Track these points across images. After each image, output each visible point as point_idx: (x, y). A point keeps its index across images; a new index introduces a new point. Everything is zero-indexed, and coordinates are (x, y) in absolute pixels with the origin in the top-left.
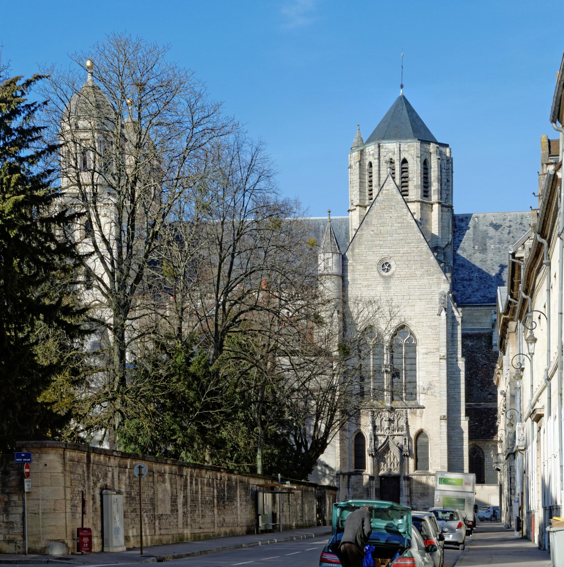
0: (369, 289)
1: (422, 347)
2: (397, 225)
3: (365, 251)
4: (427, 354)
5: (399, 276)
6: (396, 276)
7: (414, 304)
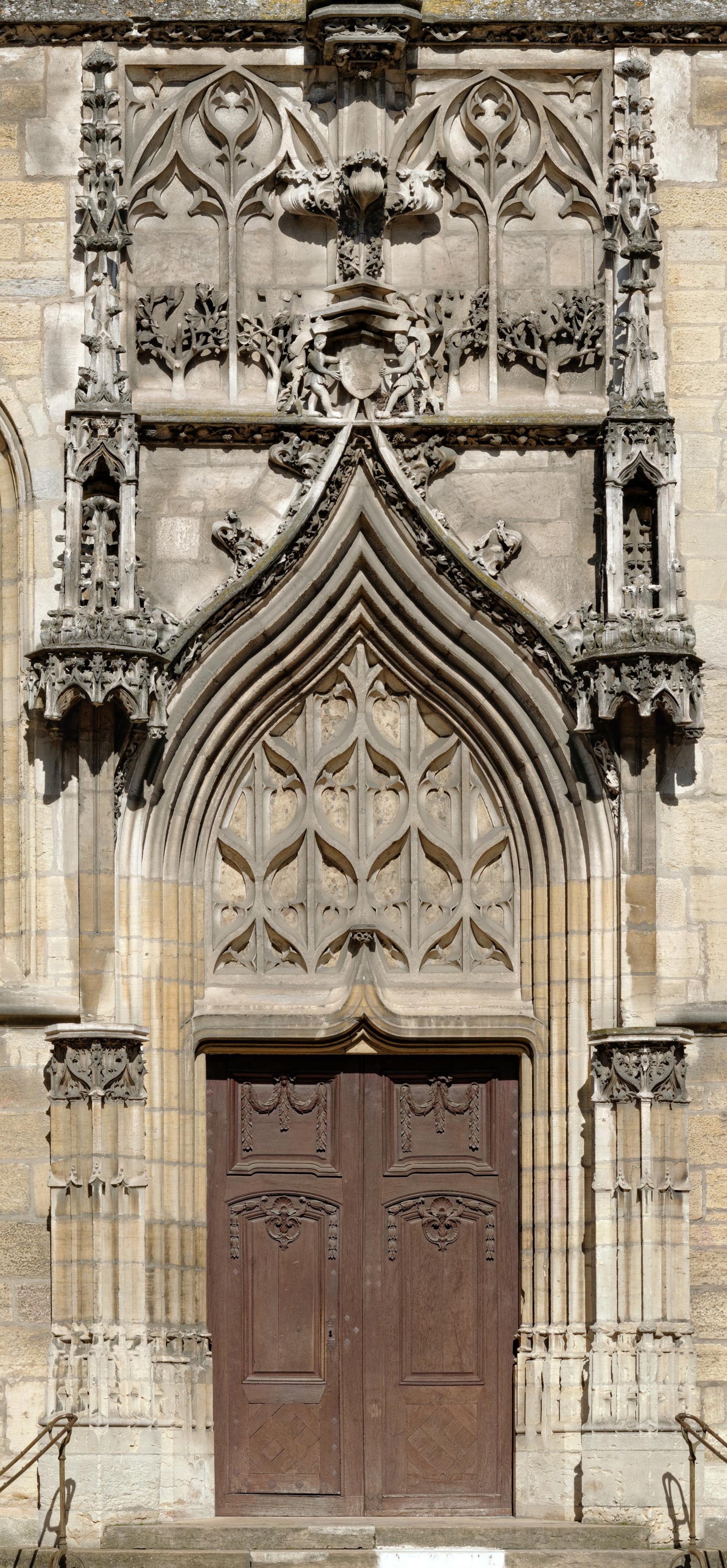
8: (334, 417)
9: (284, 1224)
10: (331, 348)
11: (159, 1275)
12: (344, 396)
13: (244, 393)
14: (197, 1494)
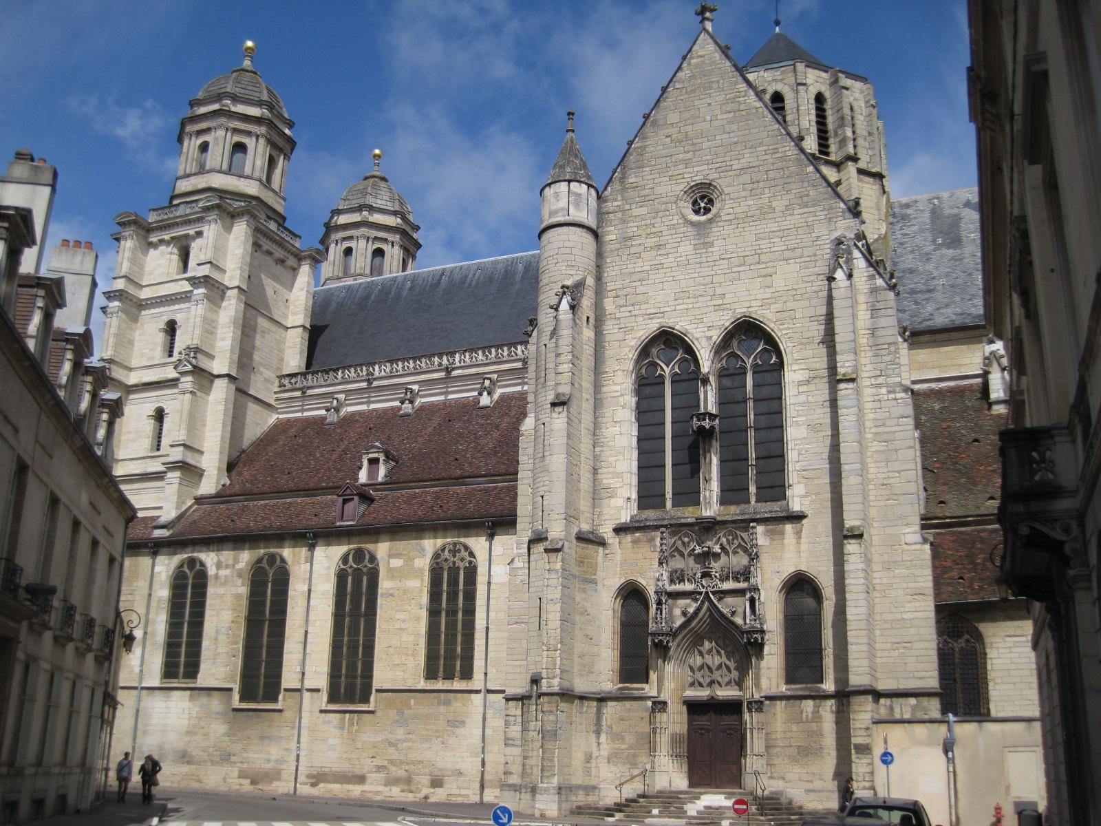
0: (661, 252)
2: (725, 116)
3: (650, 177)
4: (808, 382)
5: (731, 217)
6: (724, 218)
7: (769, 271)
9: (702, 734)
12: (703, 587)
13: (688, 587)
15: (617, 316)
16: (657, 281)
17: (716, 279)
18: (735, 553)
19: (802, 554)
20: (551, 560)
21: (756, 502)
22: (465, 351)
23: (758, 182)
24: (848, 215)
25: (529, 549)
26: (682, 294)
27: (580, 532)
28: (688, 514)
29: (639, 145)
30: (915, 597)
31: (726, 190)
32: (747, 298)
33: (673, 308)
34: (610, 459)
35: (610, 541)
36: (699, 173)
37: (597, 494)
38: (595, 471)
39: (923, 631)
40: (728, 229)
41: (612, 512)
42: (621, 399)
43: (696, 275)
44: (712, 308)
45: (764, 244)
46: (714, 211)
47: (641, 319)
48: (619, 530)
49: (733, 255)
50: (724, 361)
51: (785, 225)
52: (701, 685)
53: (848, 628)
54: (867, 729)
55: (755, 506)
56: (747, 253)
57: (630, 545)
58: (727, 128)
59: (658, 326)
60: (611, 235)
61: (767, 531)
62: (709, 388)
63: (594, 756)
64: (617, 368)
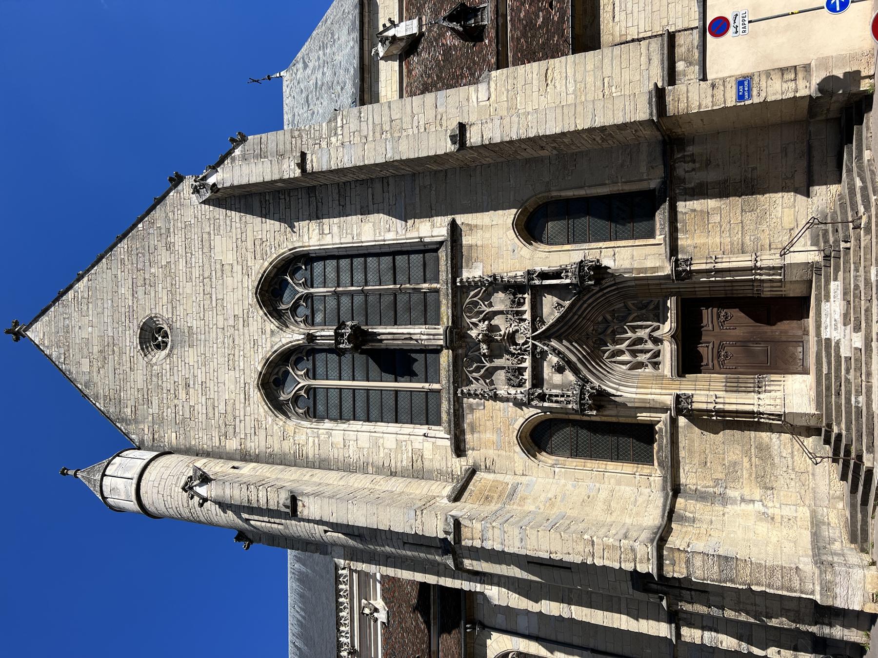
0: (192, 383)
1: (306, 237)
2: (90, 312)
3: (129, 392)
7: (218, 266)
8: (530, 344)
10: (517, 344)
11: (740, 389)
12: (526, 343)
13: (527, 364)
14: (804, 381)
15: (243, 436)
16: (216, 389)
17: (220, 325)
18: (490, 305)
19: (494, 223)
20: (469, 535)
21: (438, 283)
22: (338, 630)
23: (145, 279)
24: (180, 187)
25: (304, 520)
26: (231, 362)
27: (449, 497)
28: (445, 358)
29: (102, 402)
30: (549, 82)
31: (148, 312)
32: (240, 291)
33: (242, 373)
34: (382, 455)
35: (471, 462)
36: (131, 339)
37: (417, 472)
38: (393, 474)
39: (590, 67)
40: (180, 310)
41: (437, 457)
42: (322, 437)
43: (215, 345)
44: (246, 329)
45: (196, 273)
46: (166, 328)
47: (248, 408)
48: (459, 450)
49: (202, 306)
50: (299, 319)
51: (182, 251)
52: (657, 354)
53: (572, 129)
54: (713, 86)
55: (442, 285)
56: (202, 288)
57: (476, 435)
58: (100, 310)
59: (256, 390)
60: (171, 437)
61: (467, 266)
62: (318, 334)
63: (763, 509)
64: (292, 440)
